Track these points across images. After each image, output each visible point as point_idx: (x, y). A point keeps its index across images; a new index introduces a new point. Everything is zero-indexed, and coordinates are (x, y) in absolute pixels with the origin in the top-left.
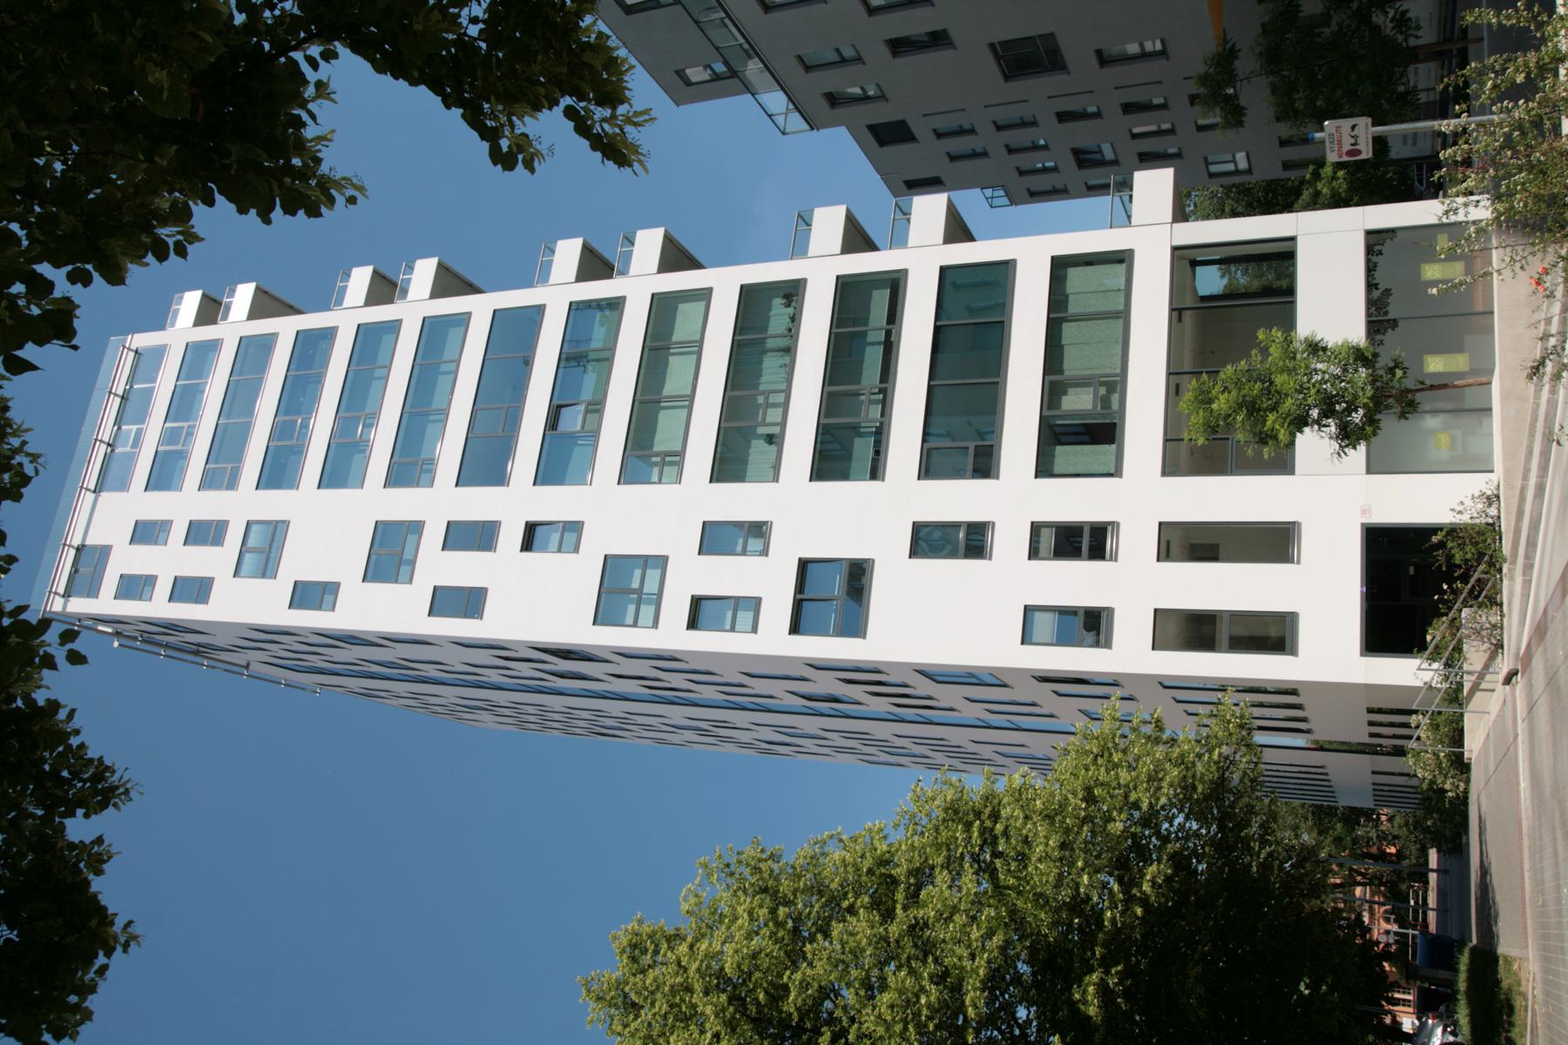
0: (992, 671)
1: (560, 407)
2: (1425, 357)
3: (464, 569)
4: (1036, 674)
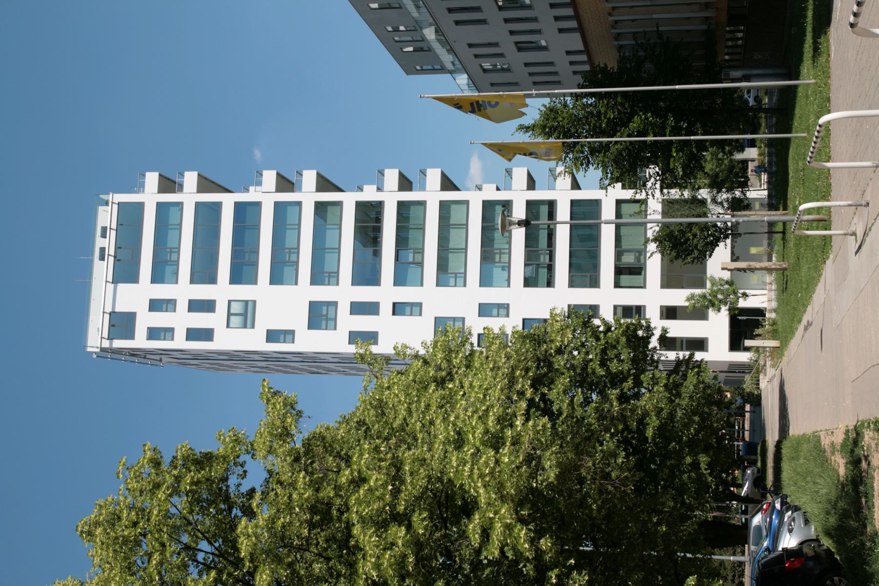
1: (398, 250)
3: (364, 323)
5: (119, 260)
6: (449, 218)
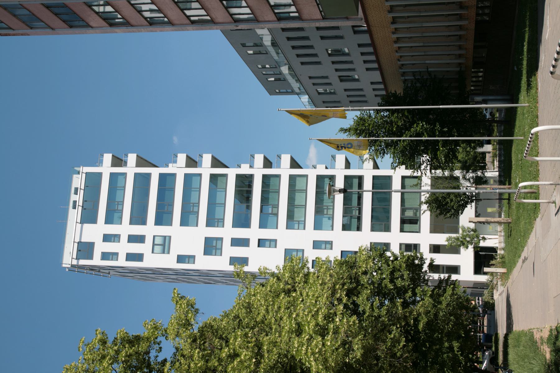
1: (262, 205)
3: (240, 252)
5: (85, 209)
6: (295, 186)
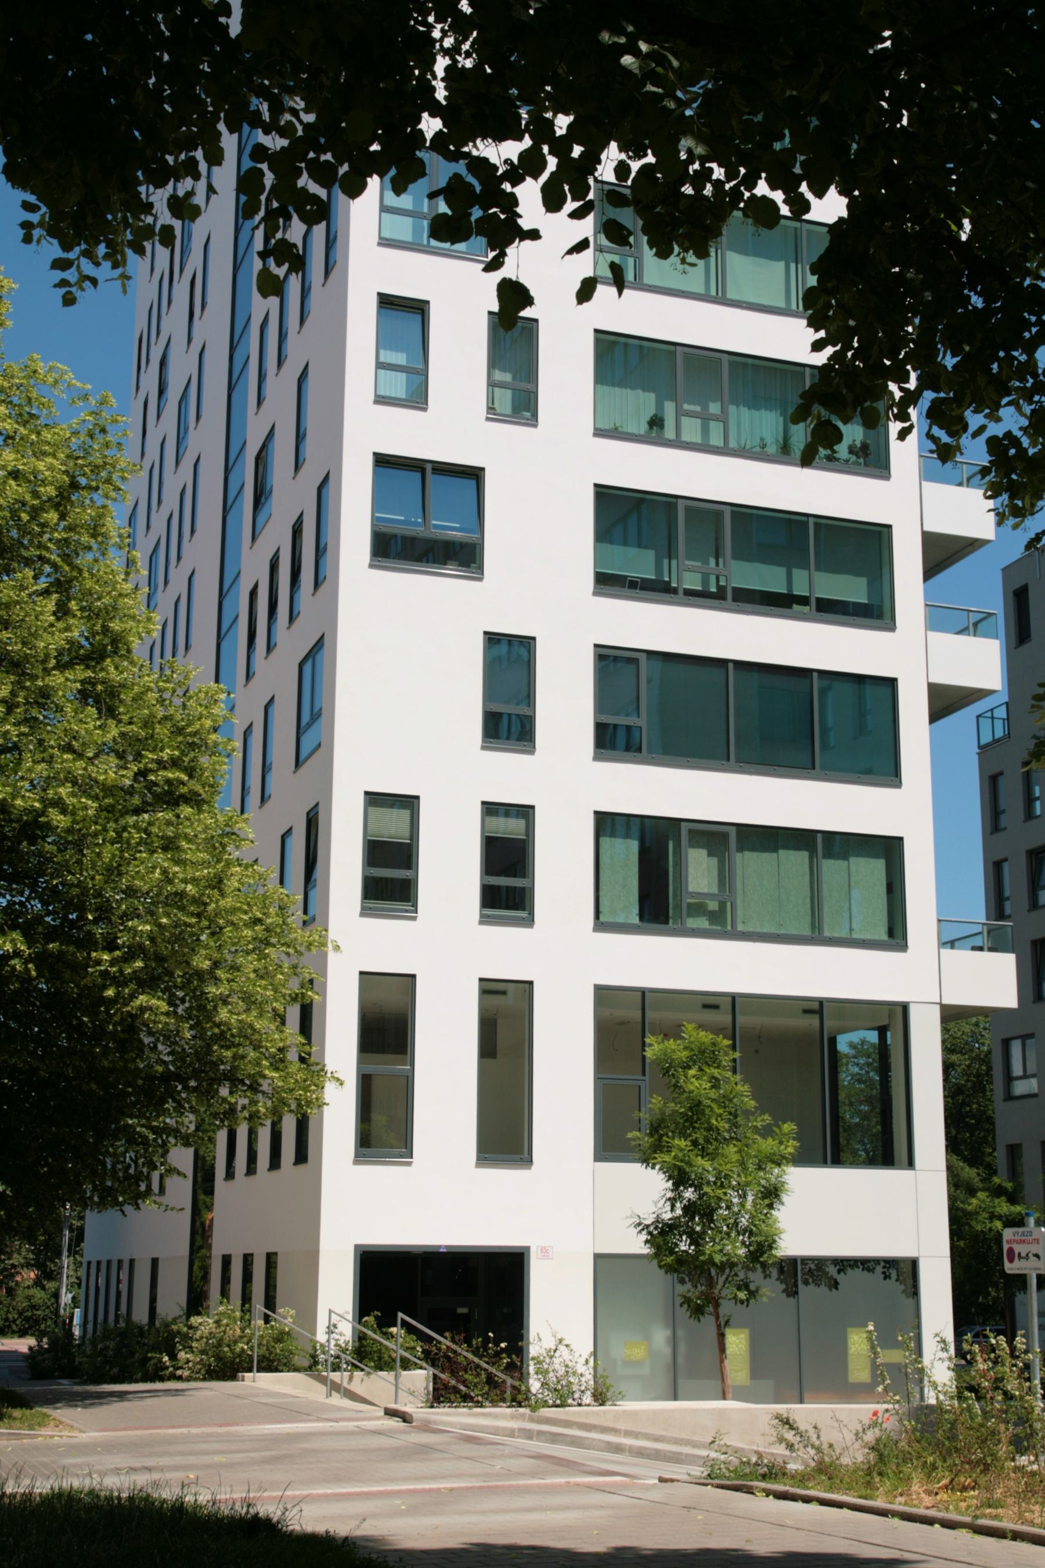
0: (323, 748)
2: (747, 1331)
4: (321, 808)
